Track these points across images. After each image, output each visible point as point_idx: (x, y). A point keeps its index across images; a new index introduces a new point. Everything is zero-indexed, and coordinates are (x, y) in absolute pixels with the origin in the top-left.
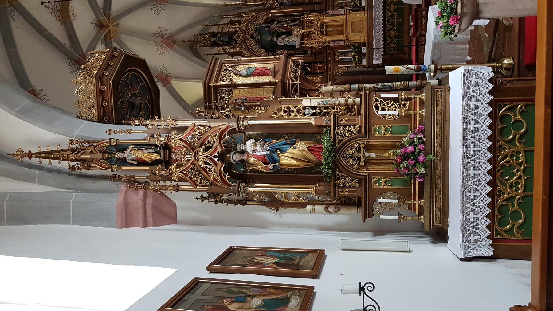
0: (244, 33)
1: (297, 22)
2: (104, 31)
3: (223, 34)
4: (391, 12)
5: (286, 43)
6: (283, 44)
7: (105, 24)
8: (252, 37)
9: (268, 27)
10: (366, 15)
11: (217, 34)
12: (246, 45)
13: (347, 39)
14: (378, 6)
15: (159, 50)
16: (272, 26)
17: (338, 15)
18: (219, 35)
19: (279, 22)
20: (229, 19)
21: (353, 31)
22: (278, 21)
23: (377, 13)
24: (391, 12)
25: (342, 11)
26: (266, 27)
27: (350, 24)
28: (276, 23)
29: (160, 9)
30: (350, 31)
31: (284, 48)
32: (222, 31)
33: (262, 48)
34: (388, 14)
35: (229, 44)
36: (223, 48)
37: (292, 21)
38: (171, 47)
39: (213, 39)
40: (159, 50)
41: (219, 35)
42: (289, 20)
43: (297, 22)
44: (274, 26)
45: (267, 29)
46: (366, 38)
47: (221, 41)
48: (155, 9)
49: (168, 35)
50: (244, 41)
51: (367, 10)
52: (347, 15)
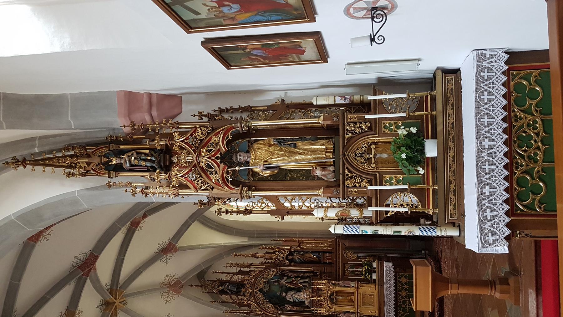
0: (253, 285)
1: (307, 280)
2: (110, 311)
3: (231, 282)
4: (402, 297)
5: (295, 299)
6: (292, 301)
7: (111, 301)
8: (261, 291)
9: (278, 281)
10: (377, 289)
11: (226, 282)
12: (255, 298)
13: (358, 313)
14: (389, 293)
15: (166, 299)
16: (282, 282)
18: (228, 284)
19: (289, 277)
20: (239, 269)
21: (364, 304)
22: (287, 276)
23: (389, 300)
24: (402, 297)
25: (352, 284)
26: (275, 282)
27: (360, 297)
28: (285, 278)
29: (168, 257)
30: (360, 303)
31: (294, 304)
32: (231, 279)
33: (270, 302)
34: (400, 313)
35: (237, 293)
36: (231, 297)
37: (302, 278)
38: (178, 293)
39: (221, 288)
40: (166, 299)
41: (228, 284)
42: (299, 277)
43: (307, 280)
44: (283, 282)
45: (276, 284)
46: (377, 312)
47: (228, 289)
48: (164, 260)
50: (252, 294)
51: (379, 286)
52: (358, 288)
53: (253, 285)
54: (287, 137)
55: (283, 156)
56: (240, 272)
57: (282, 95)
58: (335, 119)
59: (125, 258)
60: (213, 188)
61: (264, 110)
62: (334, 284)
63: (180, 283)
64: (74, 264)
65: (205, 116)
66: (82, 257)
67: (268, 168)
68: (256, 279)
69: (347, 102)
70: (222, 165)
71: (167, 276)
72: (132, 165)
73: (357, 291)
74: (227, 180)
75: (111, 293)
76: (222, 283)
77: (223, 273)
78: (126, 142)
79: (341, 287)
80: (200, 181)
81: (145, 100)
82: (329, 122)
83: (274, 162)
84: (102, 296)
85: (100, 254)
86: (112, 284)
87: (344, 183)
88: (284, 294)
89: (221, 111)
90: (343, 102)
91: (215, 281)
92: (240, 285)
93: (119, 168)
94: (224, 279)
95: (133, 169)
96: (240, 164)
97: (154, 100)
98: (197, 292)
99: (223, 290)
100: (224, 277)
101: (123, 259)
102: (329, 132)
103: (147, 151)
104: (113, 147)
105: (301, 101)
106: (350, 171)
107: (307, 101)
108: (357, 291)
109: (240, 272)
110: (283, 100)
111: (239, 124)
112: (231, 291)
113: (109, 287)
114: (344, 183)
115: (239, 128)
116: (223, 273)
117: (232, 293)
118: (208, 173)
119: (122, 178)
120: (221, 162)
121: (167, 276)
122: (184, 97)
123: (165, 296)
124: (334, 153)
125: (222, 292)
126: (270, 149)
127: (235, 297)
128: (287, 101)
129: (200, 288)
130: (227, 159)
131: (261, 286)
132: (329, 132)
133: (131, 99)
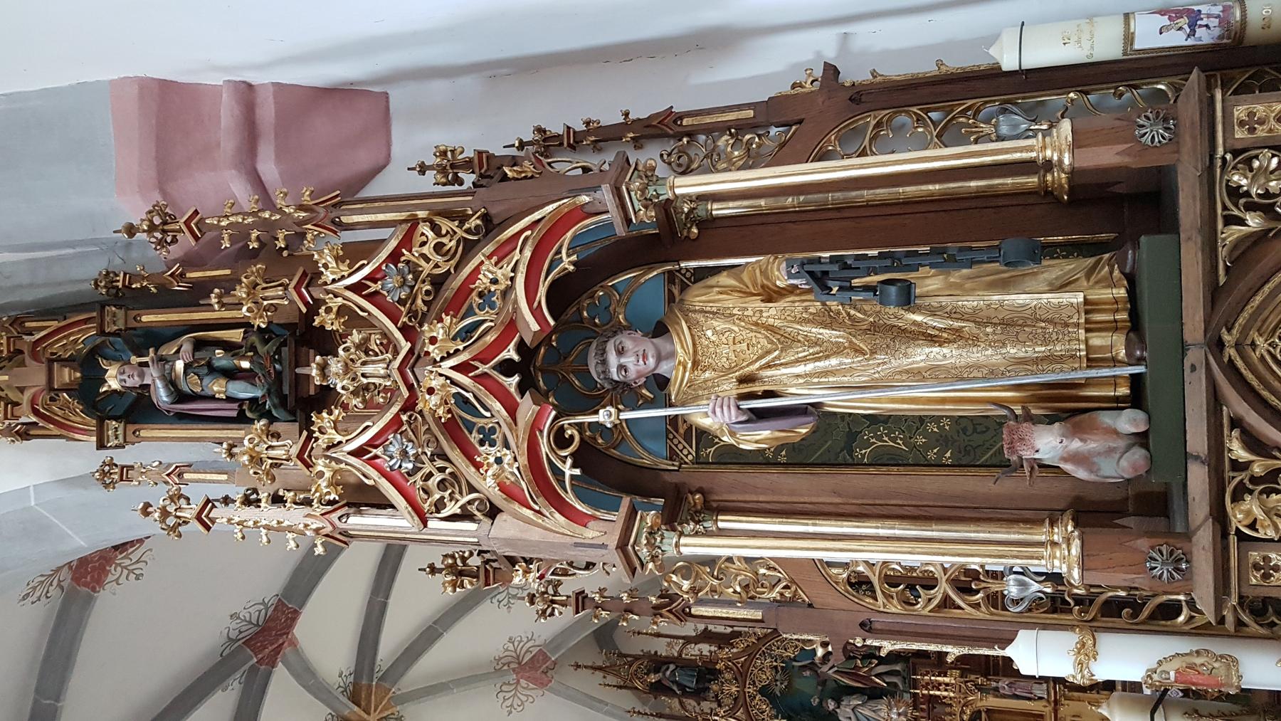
0: (742, 676)
1: (898, 668)
3: (681, 663)
8: (764, 691)
11: (667, 661)
15: (508, 703)
17: (1029, 699)
18: (672, 667)
20: (701, 627)
35: (699, 694)
36: (681, 703)
38: (542, 685)
39: (653, 678)
40: (508, 703)
41: (672, 667)
45: (807, 673)
48: (500, 597)
49: (535, 650)
52: (1056, 702)
53: (742, 676)
54: (863, 251)
55: (837, 350)
56: (706, 636)
57: (819, 47)
58: (1153, 133)
59: (391, 601)
60: (493, 512)
61: (739, 128)
62: (980, 688)
63: (546, 658)
64: (233, 635)
65: (468, 165)
66: (254, 613)
67: (760, 416)
68: (751, 657)
69: (1205, 37)
70: (527, 407)
71: (511, 640)
72: (181, 396)
73: (1056, 711)
74: (559, 474)
75: (355, 699)
76: (658, 663)
77: (658, 635)
78: (165, 299)
79: (1004, 696)
80: (438, 477)
81: (227, 114)
82: (1106, 156)
83: (798, 381)
84: (328, 705)
85: (302, 605)
86: (358, 672)
87: (1220, 516)
88: (831, 705)
89: (547, 143)
90: (1177, 39)
91: (636, 658)
92: (706, 673)
93: (137, 410)
94: (663, 652)
95: (187, 410)
96: (624, 394)
97: (267, 112)
98: (591, 683)
99: (659, 682)
100: (661, 648)
101: (384, 606)
102: (1112, 214)
103: (236, 335)
104: (117, 319)
105: (927, 68)
106: (1254, 443)
107: (957, 62)
108: (1056, 711)
109: (706, 636)
110: (831, 71)
111: (606, 195)
112: (682, 687)
113: (351, 679)
114: (1220, 516)
115: (614, 215)
116: (658, 635)
117: (685, 692)
118: (474, 438)
119: (155, 448)
120: (522, 389)
121: (511, 640)
122: (398, 97)
123: (508, 695)
124: (1135, 326)
125: (658, 689)
126: (772, 313)
127: (693, 703)
128: (853, 74)
129: (599, 674)
130: (553, 368)
131: (765, 677)
132: (1112, 214)
133: (167, 107)
